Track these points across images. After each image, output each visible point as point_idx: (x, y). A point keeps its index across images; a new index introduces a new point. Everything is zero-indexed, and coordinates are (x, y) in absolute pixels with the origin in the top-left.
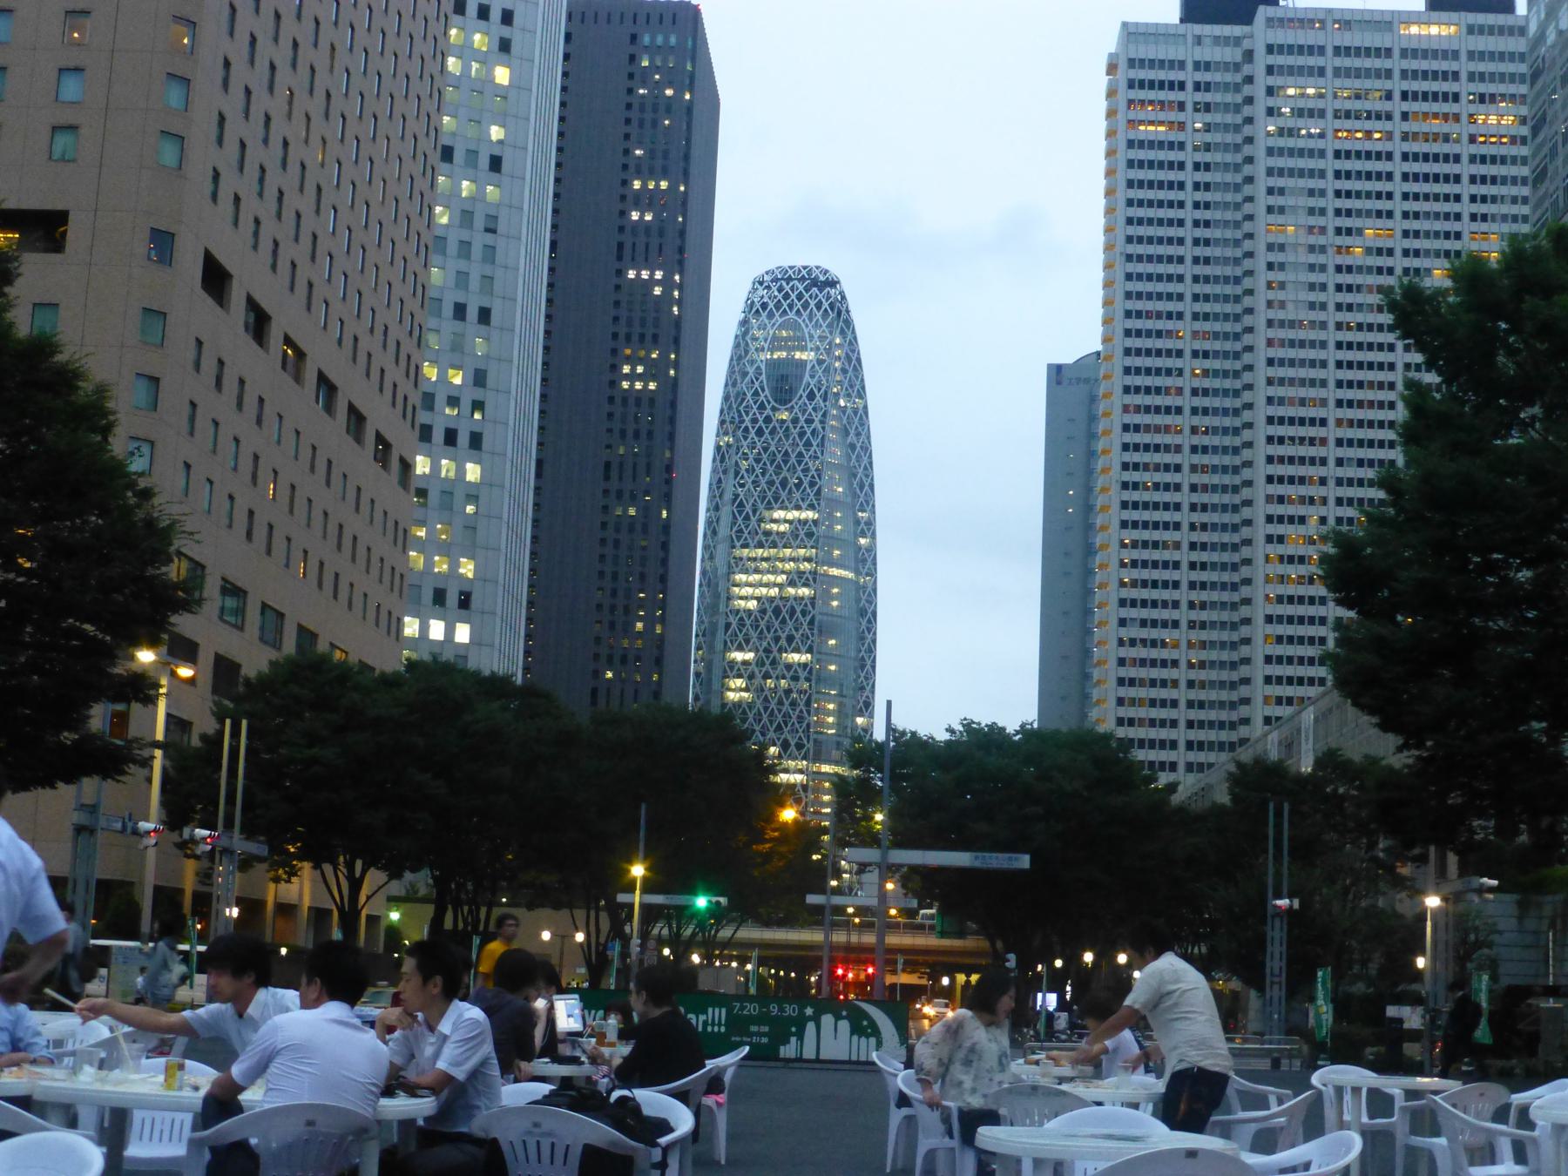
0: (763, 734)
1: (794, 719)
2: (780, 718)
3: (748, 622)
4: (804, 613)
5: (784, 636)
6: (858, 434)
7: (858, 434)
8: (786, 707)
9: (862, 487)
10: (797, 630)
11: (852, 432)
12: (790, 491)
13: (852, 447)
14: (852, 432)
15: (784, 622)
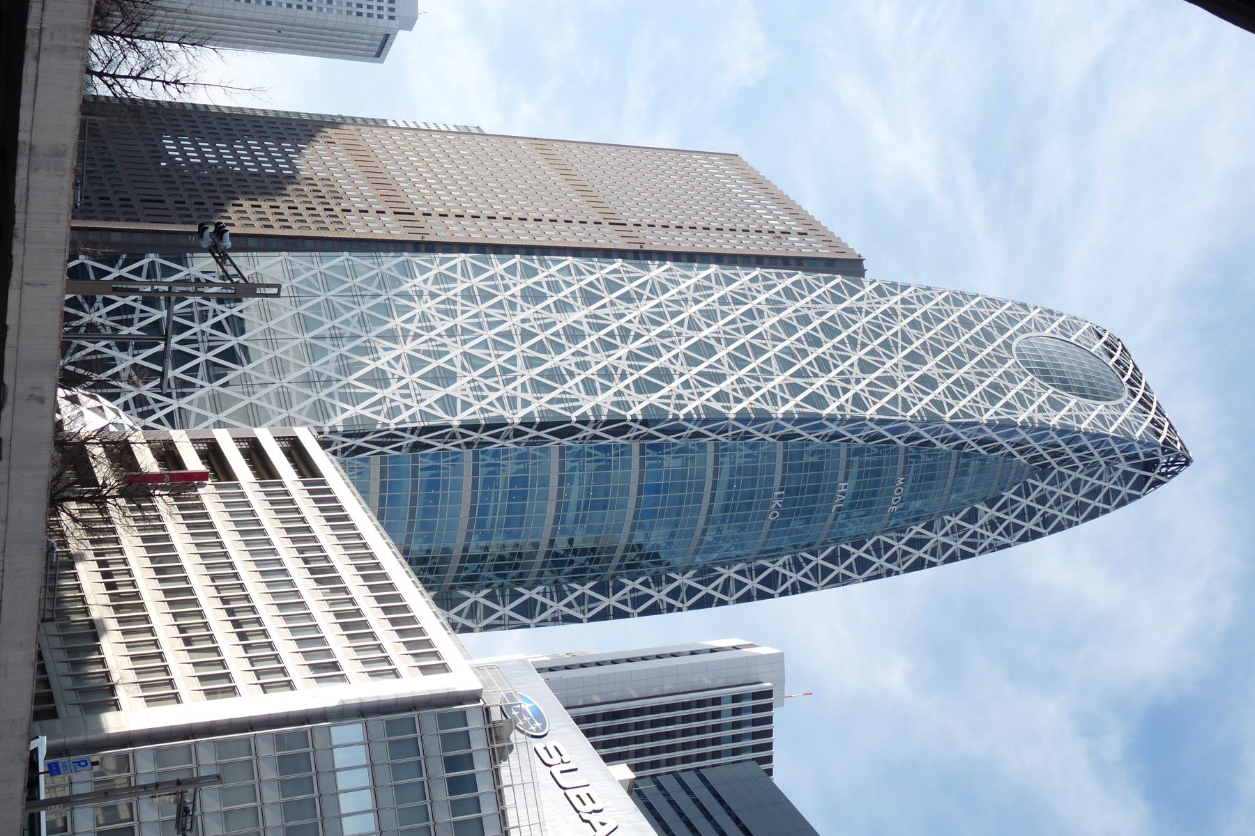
0: (451, 332)
1: (504, 391)
2: (494, 363)
3: (663, 298)
4: (720, 396)
5: (662, 361)
6: (993, 525)
7: (993, 525)
8: (527, 375)
9: (917, 543)
10: (686, 385)
11: (993, 512)
12: (907, 368)
13: (972, 517)
14: (993, 512)
15: (692, 362)
